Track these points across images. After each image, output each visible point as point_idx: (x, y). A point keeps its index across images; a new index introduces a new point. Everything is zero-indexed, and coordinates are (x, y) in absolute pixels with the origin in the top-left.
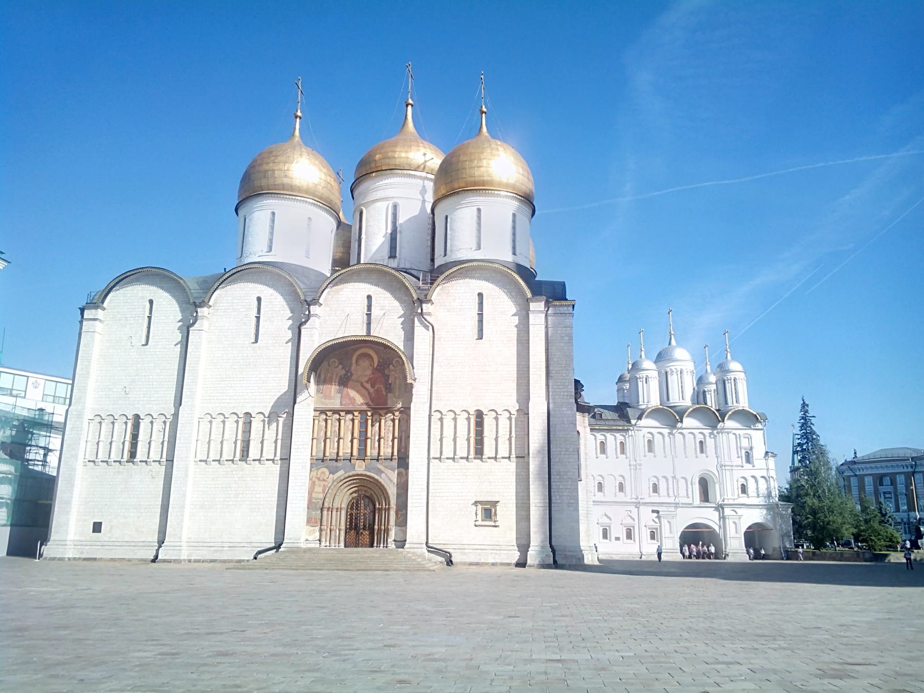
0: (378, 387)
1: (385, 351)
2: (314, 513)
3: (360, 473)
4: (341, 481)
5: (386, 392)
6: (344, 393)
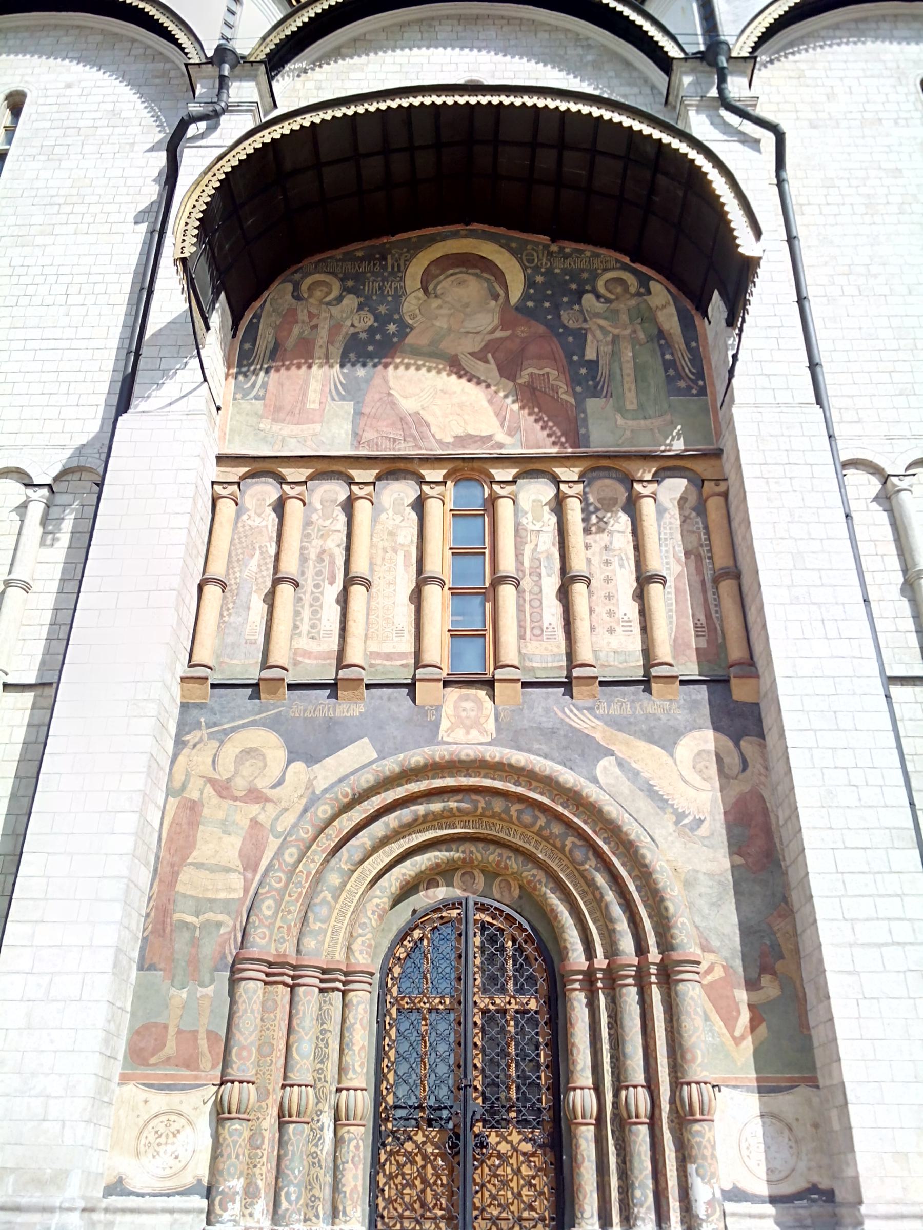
0: (531, 375)
1: (554, 248)
2: (184, 994)
3: (468, 753)
4: (347, 807)
5: (575, 395)
6: (372, 397)
